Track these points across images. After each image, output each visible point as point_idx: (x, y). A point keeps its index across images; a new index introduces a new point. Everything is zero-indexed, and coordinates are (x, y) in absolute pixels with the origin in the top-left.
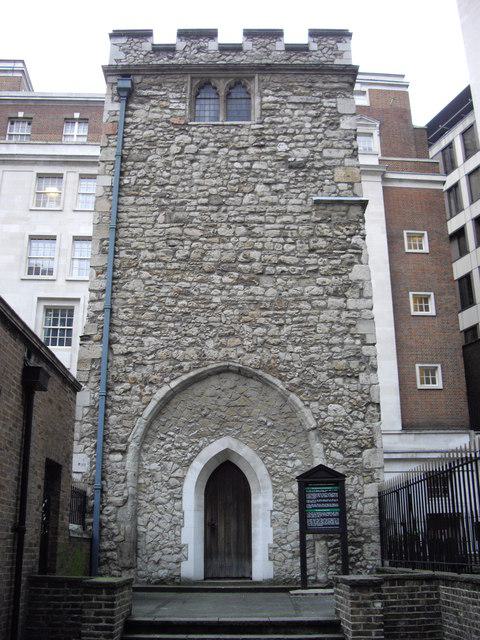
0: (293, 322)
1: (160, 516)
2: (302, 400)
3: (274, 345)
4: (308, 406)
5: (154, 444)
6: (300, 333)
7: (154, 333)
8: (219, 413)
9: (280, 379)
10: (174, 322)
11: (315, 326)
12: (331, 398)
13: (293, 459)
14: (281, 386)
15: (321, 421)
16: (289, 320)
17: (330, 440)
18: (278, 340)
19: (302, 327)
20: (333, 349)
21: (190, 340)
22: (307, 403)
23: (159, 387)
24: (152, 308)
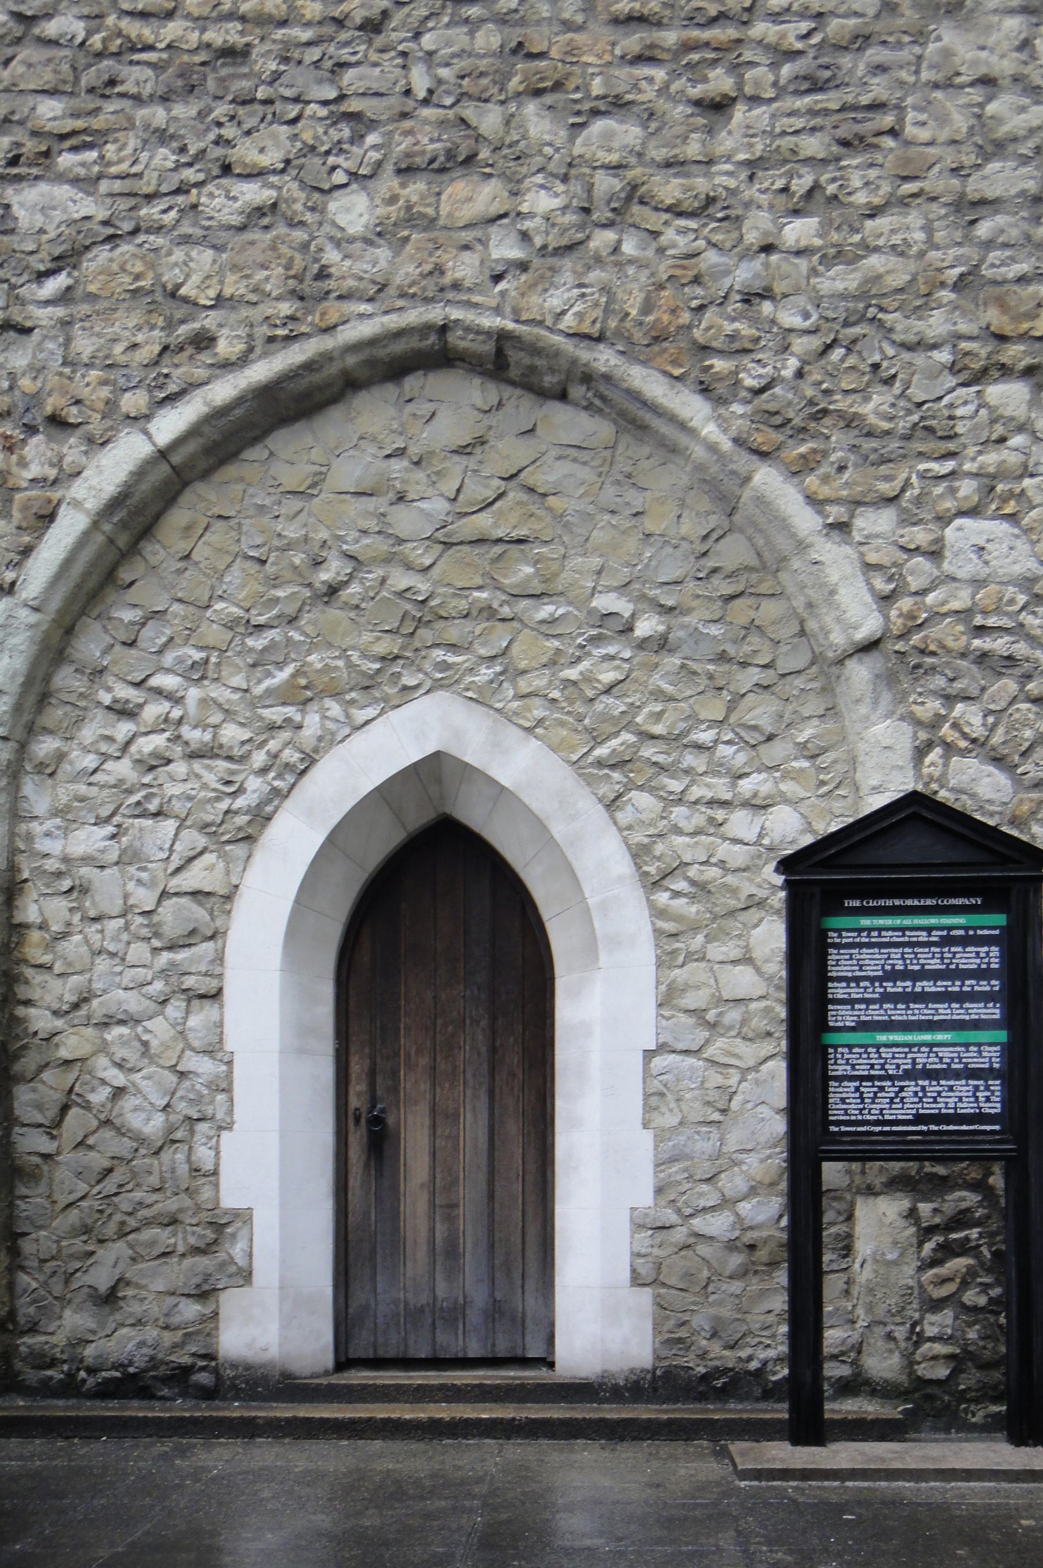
0: (781, 91)
1: (119, 1078)
2: (814, 501)
3: (676, 211)
4: (842, 527)
5: (88, 733)
6: (813, 145)
7: (66, 160)
8: (401, 580)
9: (705, 390)
10: (165, 99)
11: (900, 109)
12: (967, 488)
13: (758, 806)
14: (710, 430)
15: (905, 604)
16: (758, 77)
17: (950, 699)
18: (701, 184)
19: (826, 112)
20: (983, 230)
21: (252, 193)
22: (835, 512)
23: (97, 443)
24: (51, 28)
